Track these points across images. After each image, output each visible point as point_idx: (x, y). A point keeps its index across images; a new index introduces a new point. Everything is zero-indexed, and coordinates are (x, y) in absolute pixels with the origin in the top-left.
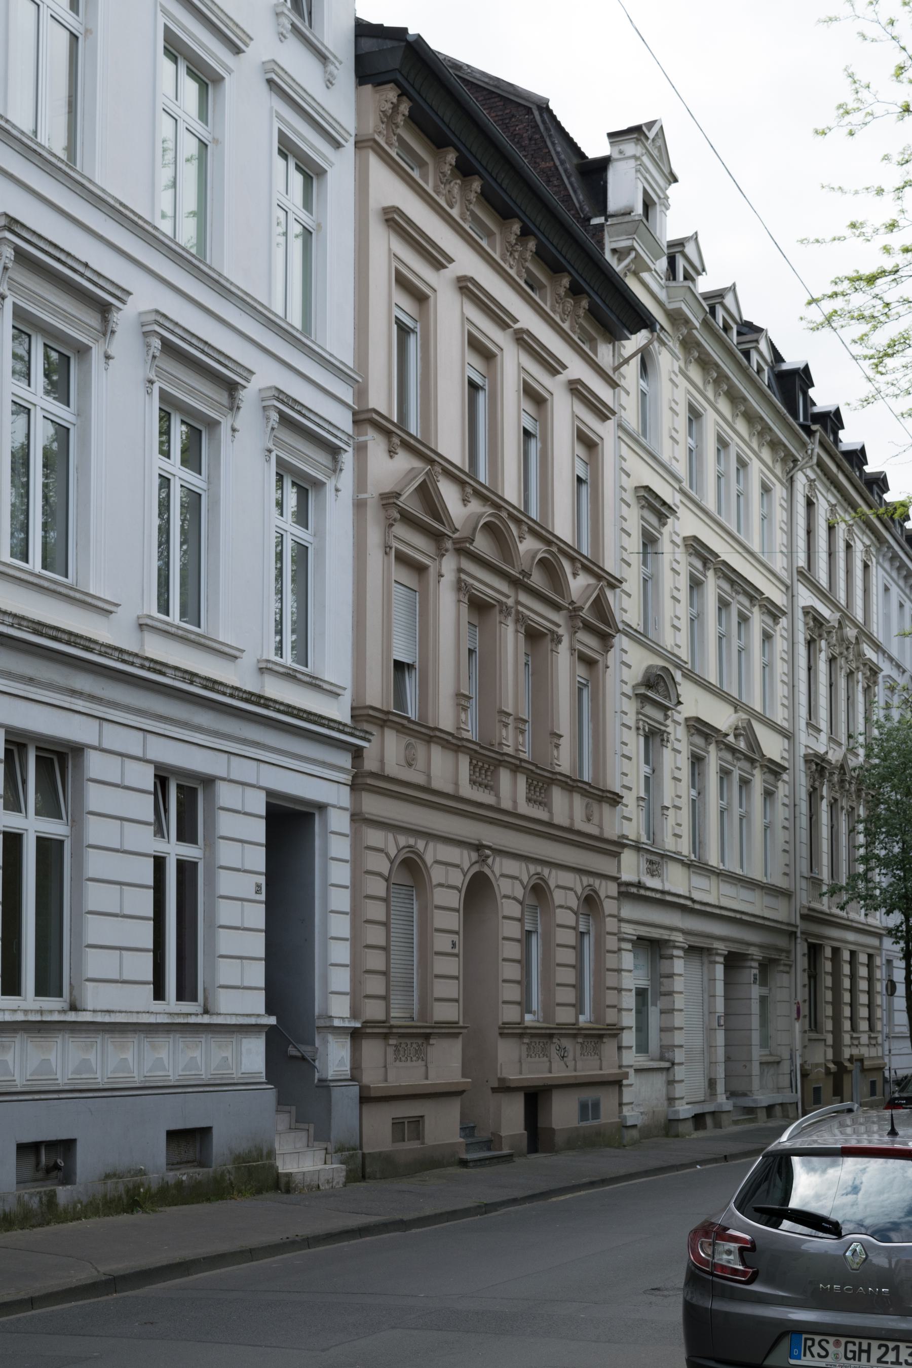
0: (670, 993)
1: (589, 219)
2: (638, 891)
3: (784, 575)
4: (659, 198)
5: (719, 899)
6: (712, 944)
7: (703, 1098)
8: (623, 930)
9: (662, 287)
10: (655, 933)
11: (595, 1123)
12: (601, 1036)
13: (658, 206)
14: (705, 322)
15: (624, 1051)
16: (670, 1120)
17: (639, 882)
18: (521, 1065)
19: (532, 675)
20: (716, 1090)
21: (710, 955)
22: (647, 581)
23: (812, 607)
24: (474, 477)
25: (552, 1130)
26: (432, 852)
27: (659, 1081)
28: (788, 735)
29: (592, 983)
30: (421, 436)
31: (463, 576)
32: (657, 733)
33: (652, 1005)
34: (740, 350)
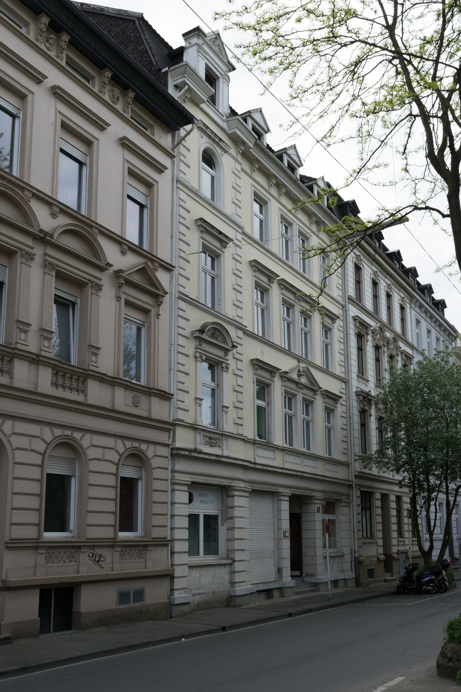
0: (232, 518)
1: (161, 70)
2: (190, 453)
3: (340, 300)
4: (222, 75)
5: (283, 464)
6: (278, 490)
7: (274, 580)
8: (176, 478)
9: (224, 121)
10: (226, 482)
11: (138, 604)
12: (146, 546)
13: (221, 79)
14: (256, 145)
15: (176, 555)
16: (231, 596)
17: (196, 449)
18: (36, 569)
19: (80, 310)
20: (282, 575)
21: (278, 496)
22: (214, 278)
23: (357, 316)
24: (78, 212)
25: (80, 613)
26: (150, 451)
27: (223, 573)
28: (345, 381)
29: (143, 511)
30: (19, 176)
31: (47, 258)
32: (220, 363)
33: (221, 525)
34: (306, 186)
